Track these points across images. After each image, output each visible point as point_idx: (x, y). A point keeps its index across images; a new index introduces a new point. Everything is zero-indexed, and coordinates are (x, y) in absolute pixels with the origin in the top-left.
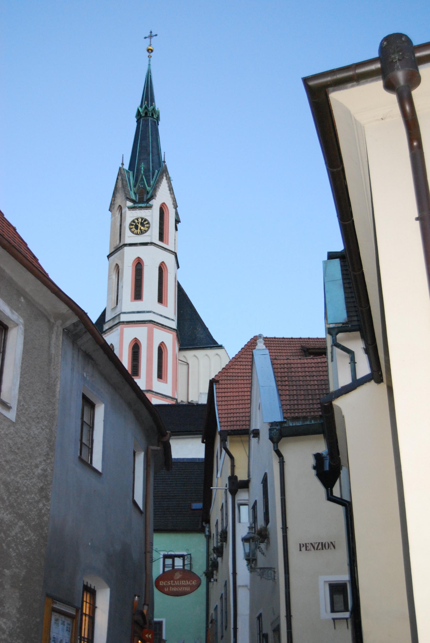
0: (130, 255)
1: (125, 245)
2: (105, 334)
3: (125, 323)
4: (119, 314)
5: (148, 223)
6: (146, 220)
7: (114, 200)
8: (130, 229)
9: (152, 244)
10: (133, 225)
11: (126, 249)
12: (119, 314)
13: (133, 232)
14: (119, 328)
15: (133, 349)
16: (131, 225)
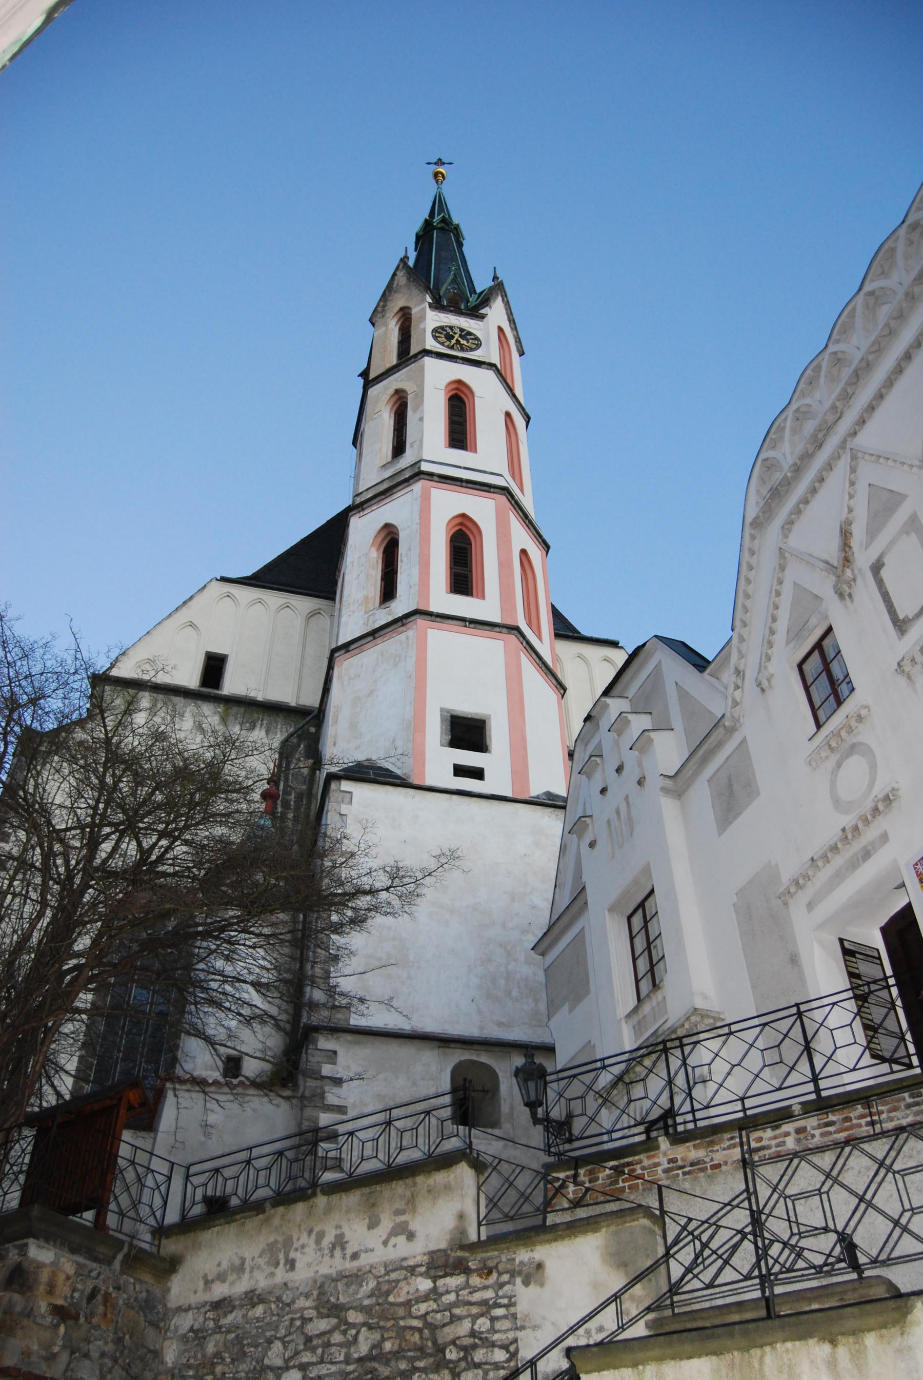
0: (436, 377)
1: (427, 352)
2: (363, 510)
3: (436, 479)
4: (420, 461)
5: (477, 339)
6: (470, 333)
7: (384, 306)
8: (435, 338)
9: (491, 366)
11: (428, 361)
12: (420, 461)
13: (442, 344)
14: (418, 487)
15: (451, 541)
16: (435, 331)
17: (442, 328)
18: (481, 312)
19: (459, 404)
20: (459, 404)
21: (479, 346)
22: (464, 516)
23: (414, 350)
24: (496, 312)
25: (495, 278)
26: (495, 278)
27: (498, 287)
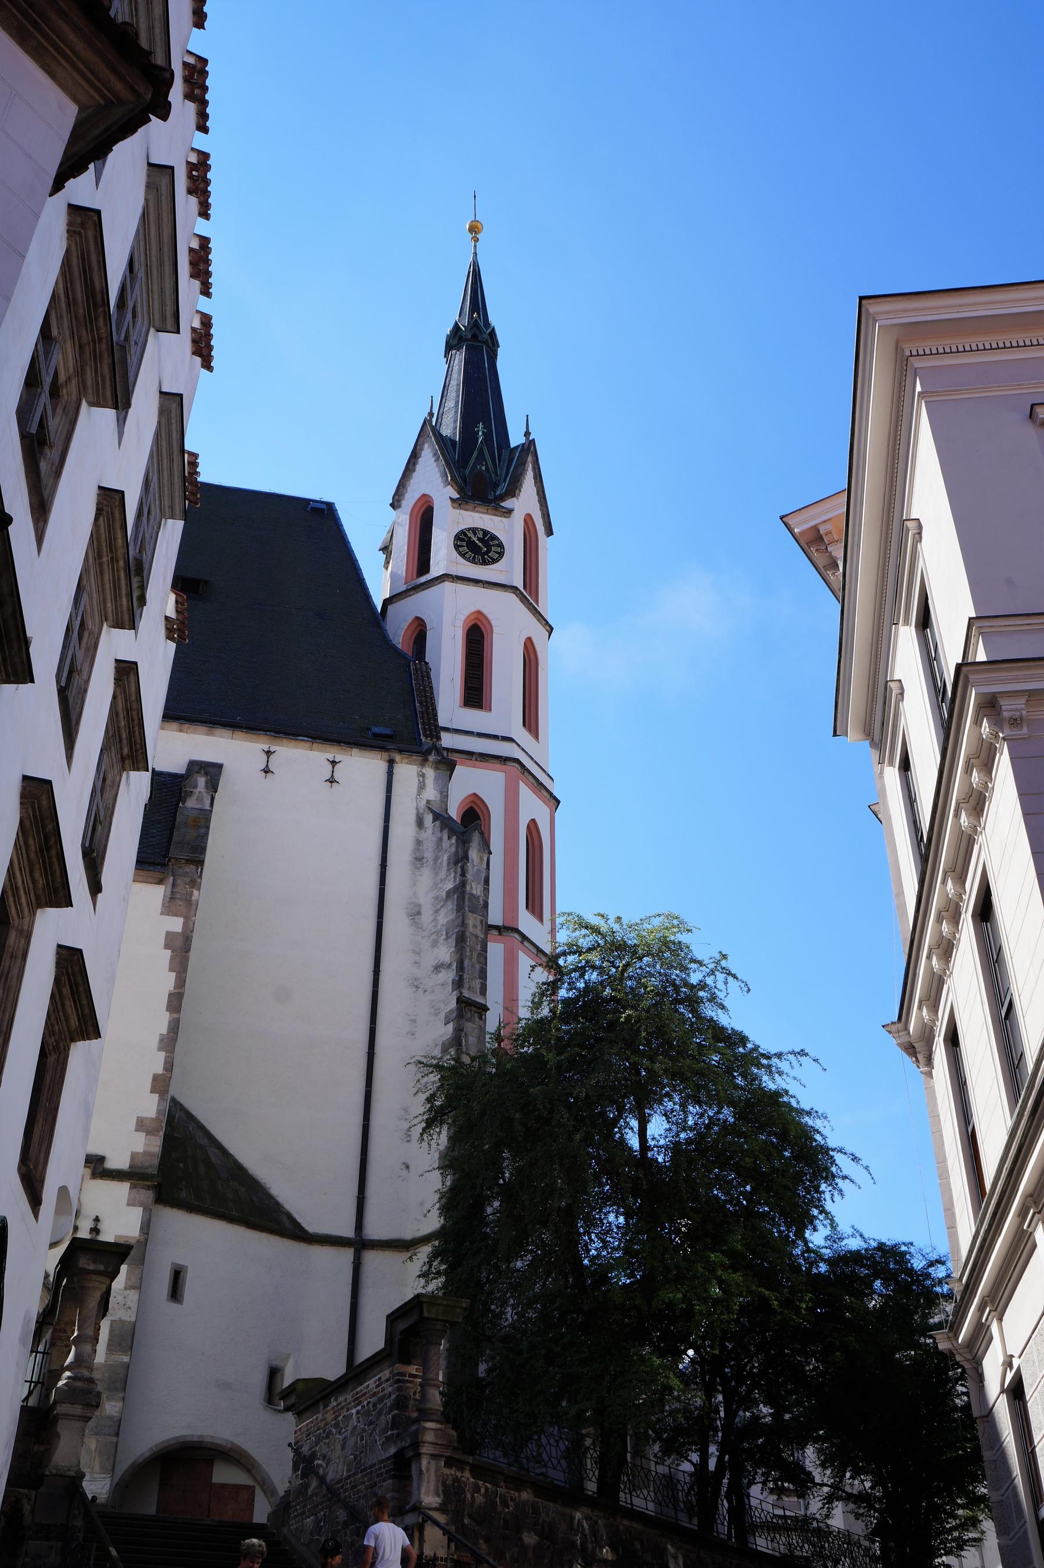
5: (501, 545)
9: (514, 589)
10: (462, 540)
11: (448, 585)
13: (463, 555)
16: (457, 537)
17: (462, 532)
18: (507, 504)
19: (477, 639)
20: (477, 639)
21: (501, 555)
22: (475, 794)
23: (435, 571)
24: (524, 502)
25: (527, 434)
26: (527, 434)
27: (529, 448)
